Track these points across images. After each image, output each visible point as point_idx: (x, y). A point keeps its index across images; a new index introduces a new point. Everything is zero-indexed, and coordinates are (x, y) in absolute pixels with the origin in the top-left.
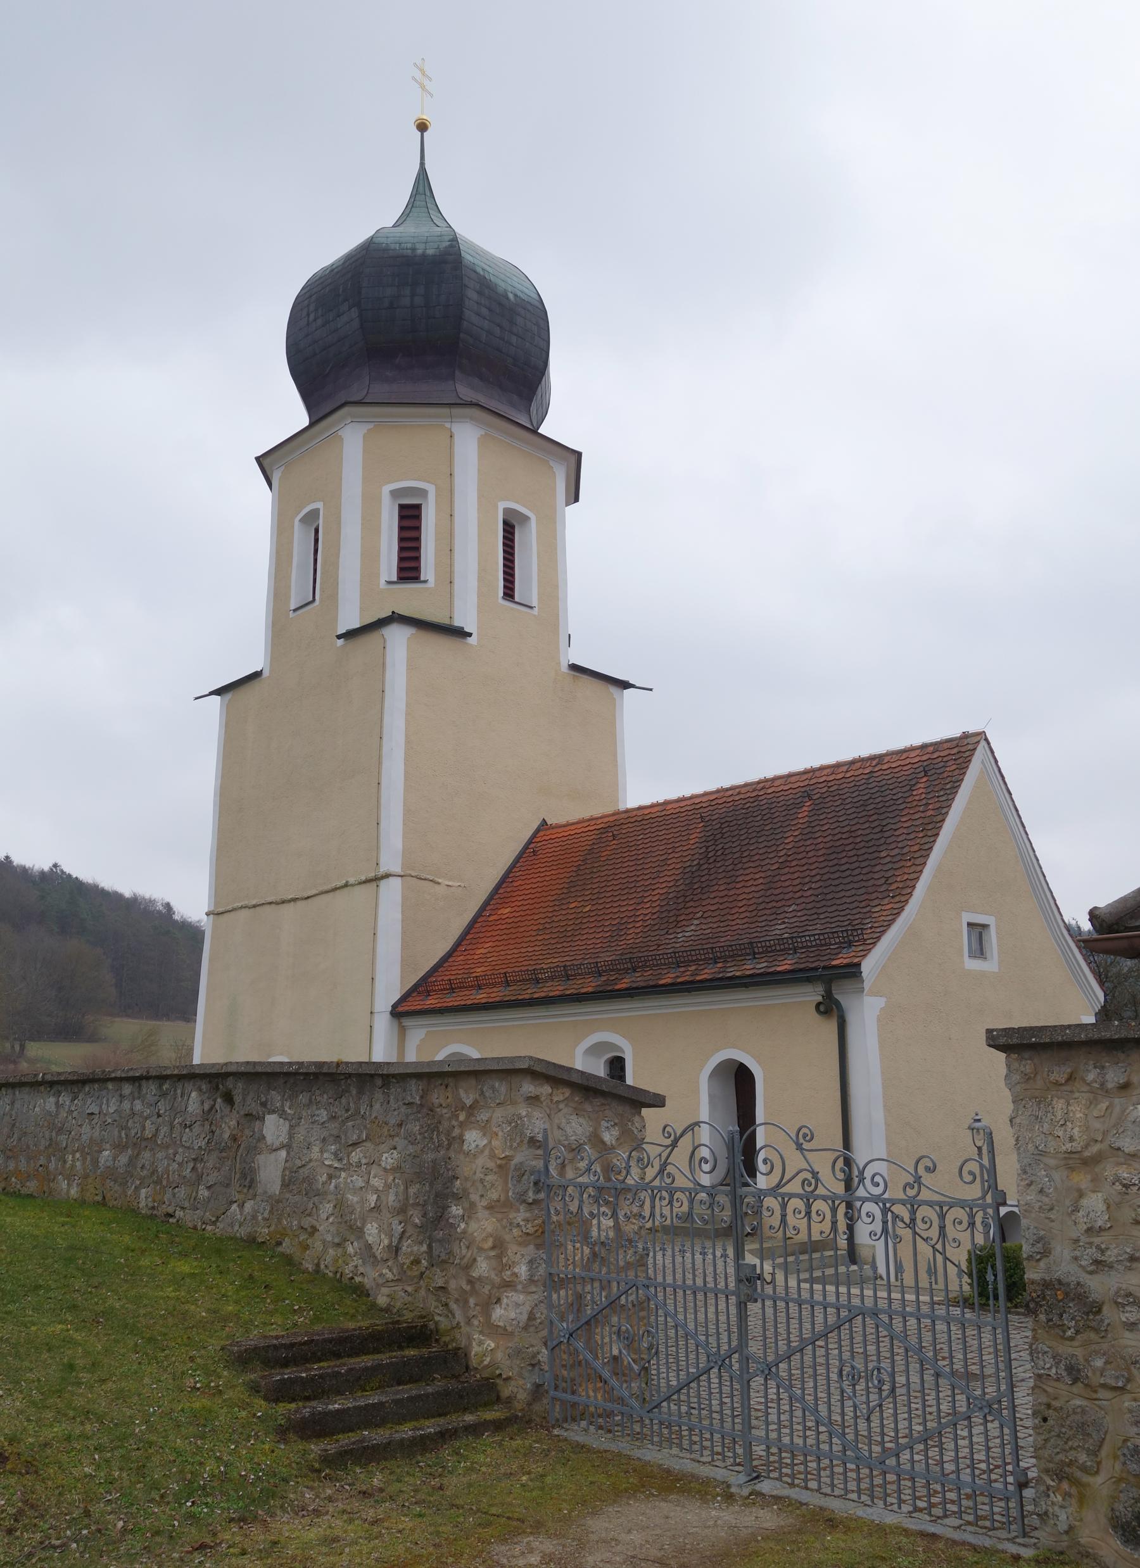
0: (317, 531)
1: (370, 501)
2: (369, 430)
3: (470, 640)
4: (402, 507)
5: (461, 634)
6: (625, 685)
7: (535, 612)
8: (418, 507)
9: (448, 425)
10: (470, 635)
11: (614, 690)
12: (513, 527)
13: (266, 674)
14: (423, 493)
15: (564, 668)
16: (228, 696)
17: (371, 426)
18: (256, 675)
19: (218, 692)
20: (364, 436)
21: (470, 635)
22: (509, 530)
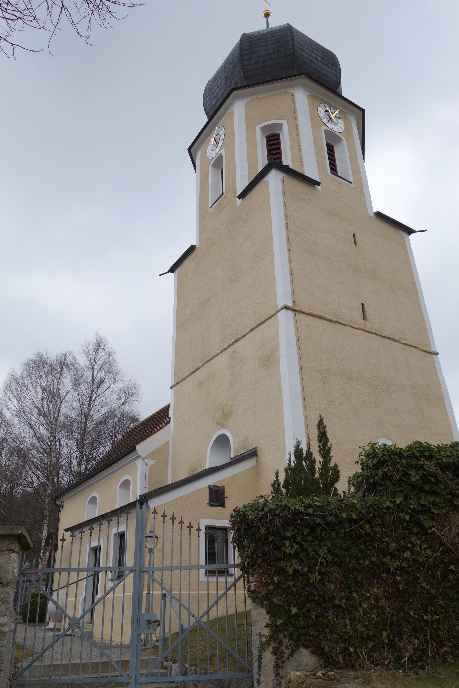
0: (222, 171)
1: (251, 140)
2: (247, 102)
3: (319, 188)
4: (267, 137)
5: (313, 183)
6: (410, 231)
7: (353, 185)
8: (278, 135)
9: (290, 91)
10: (319, 184)
11: (404, 235)
12: (332, 147)
13: (198, 246)
14: (279, 126)
15: (373, 215)
16: (177, 272)
17: (248, 100)
18: (192, 249)
19: (172, 270)
20: (245, 105)
21: (319, 184)
22: (331, 149)
